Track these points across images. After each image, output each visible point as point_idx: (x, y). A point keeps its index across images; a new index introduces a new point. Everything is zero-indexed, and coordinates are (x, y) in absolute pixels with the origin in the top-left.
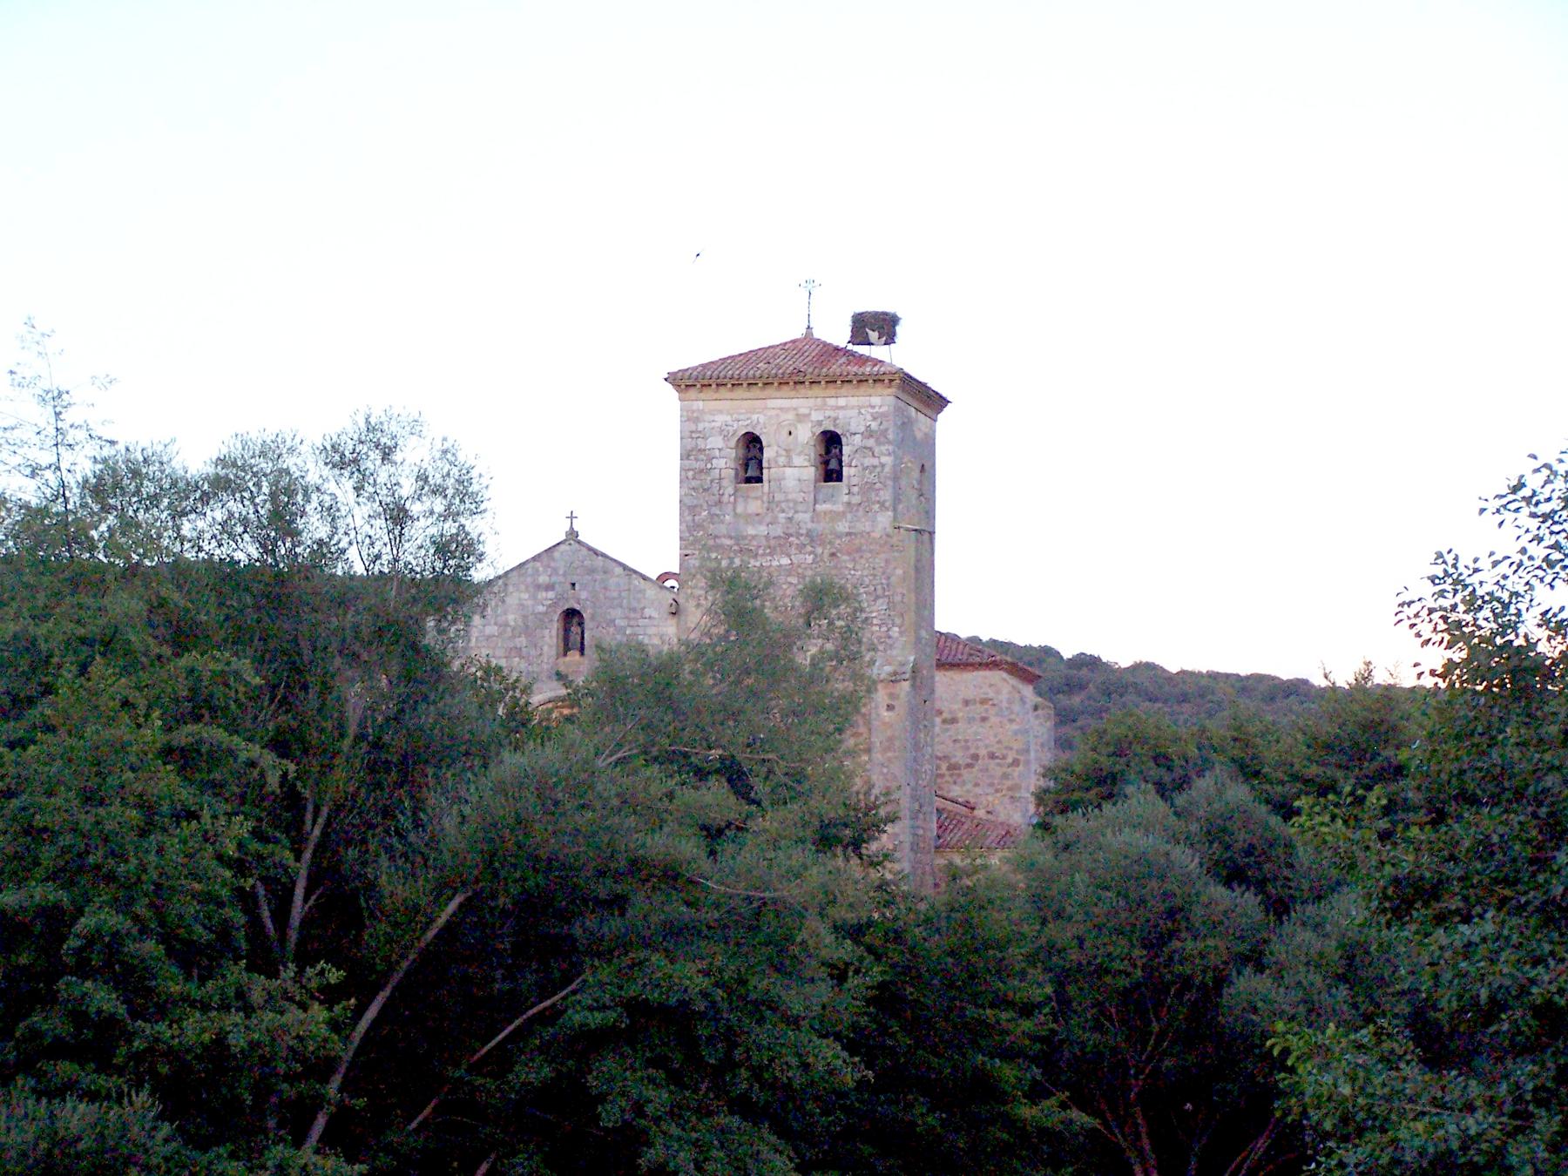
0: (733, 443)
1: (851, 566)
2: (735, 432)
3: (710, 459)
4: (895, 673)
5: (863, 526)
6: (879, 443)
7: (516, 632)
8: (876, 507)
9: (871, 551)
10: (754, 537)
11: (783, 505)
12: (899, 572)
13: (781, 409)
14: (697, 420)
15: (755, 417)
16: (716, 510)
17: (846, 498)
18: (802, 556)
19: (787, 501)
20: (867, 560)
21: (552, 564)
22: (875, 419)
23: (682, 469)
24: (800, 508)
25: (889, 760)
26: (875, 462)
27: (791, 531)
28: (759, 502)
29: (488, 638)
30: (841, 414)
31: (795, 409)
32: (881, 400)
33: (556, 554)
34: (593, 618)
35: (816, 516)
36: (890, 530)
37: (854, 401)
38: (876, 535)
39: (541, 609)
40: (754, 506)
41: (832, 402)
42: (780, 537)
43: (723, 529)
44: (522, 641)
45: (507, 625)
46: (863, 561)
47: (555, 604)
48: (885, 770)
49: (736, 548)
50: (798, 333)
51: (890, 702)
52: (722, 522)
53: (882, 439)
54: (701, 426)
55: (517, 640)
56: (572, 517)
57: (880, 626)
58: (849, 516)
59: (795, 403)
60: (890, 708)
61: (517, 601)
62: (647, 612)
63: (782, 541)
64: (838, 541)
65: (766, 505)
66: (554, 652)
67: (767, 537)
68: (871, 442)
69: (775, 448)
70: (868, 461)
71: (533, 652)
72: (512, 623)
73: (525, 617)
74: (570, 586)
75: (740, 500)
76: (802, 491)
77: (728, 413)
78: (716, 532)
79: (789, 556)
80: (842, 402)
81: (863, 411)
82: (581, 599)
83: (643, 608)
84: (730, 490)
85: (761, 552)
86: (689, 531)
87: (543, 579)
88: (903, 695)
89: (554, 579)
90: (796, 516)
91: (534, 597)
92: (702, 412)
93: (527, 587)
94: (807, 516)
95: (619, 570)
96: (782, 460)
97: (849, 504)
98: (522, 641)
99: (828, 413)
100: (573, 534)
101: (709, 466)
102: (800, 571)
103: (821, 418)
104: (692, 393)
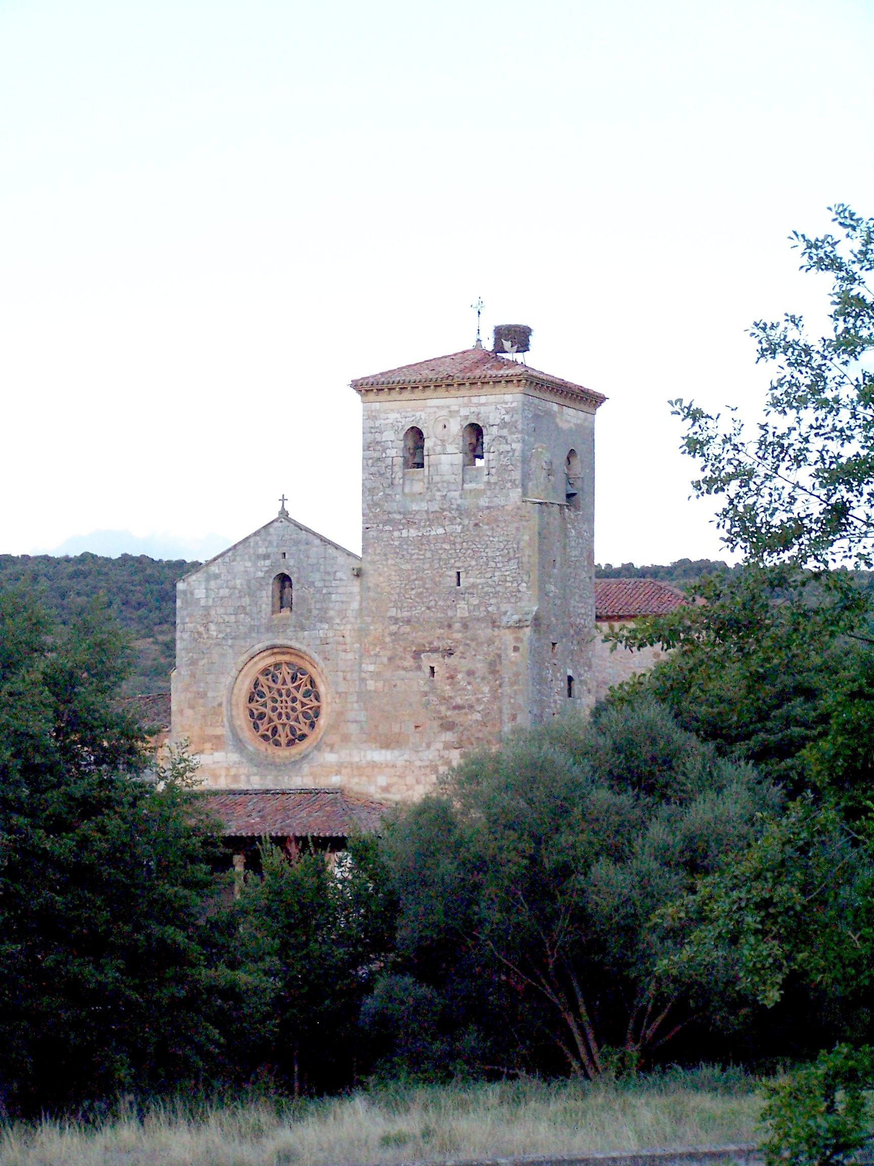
0: (401, 436)
2: (403, 426)
3: (384, 451)
4: (520, 621)
5: (499, 501)
6: (511, 433)
7: (243, 594)
8: (509, 485)
9: (505, 521)
10: (417, 512)
11: (439, 485)
12: (526, 538)
13: (438, 407)
14: (375, 418)
15: (418, 414)
16: (388, 491)
17: (486, 478)
18: (453, 527)
19: (443, 482)
20: (502, 528)
21: (269, 538)
22: (507, 413)
23: (364, 458)
24: (452, 487)
25: (515, 692)
26: (508, 448)
27: (445, 506)
28: (422, 484)
29: (222, 598)
30: (482, 409)
31: (448, 407)
32: (512, 397)
33: (271, 530)
34: (298, 581)
35: (464, 494)
36: (519, 503)
37: (491, 398)
38: (509, 508)
39: (260, 574)
40: (418, 487)
41: (475, 400)
42: (436, 512)
43: (394, 506)
44: (246, 601)
45: (235, 588)
46: (499, 530)
48: (512, 701)
49: (404, 521)
50: (469, 345)
51: (517, 645)
52: (394, 500)
53: (514, 429)
54: (377, 424)
55: (243, 600)
56: (283, 500)
57: (512, 582)
58: (488, 493)
59: (448, 401)
60: (516, 649)
61: (242, 569)
62: (339, 575)
63: (438, 515)
64: (480, 514)
65: (426, 486)
66: (269, 609)
67: (427, 512)
68: (505, 432)
69: (433, 439)
70: (504, 447)
71: (255, 610)
72: (239, 587)
73: (249, 581)
74: (281, 556)
75: (407, 482)
77: (399, 412)
78: (390, 509)
79: (444, 527)
80: (483, 399)
81: (499, 406)
82: (289, 567)
83: (336, 572)
84: (400, 475)
85: (422, 524)
86: (370, 509)
87: (262, 550)
88: (525, 638)
89: (269, 550)
90: (449, 494)
91: (255, 565)
92: (378, 411)
93: (250, 557)
94: (456, 494)
95: (317, 542)
96: (438, 449)
97: (488, 483)
98: (246, 601)
99: (473, 409)
100: (284, 514)
101: (384, 455)
102: (452, 538)
104: (371, 396)
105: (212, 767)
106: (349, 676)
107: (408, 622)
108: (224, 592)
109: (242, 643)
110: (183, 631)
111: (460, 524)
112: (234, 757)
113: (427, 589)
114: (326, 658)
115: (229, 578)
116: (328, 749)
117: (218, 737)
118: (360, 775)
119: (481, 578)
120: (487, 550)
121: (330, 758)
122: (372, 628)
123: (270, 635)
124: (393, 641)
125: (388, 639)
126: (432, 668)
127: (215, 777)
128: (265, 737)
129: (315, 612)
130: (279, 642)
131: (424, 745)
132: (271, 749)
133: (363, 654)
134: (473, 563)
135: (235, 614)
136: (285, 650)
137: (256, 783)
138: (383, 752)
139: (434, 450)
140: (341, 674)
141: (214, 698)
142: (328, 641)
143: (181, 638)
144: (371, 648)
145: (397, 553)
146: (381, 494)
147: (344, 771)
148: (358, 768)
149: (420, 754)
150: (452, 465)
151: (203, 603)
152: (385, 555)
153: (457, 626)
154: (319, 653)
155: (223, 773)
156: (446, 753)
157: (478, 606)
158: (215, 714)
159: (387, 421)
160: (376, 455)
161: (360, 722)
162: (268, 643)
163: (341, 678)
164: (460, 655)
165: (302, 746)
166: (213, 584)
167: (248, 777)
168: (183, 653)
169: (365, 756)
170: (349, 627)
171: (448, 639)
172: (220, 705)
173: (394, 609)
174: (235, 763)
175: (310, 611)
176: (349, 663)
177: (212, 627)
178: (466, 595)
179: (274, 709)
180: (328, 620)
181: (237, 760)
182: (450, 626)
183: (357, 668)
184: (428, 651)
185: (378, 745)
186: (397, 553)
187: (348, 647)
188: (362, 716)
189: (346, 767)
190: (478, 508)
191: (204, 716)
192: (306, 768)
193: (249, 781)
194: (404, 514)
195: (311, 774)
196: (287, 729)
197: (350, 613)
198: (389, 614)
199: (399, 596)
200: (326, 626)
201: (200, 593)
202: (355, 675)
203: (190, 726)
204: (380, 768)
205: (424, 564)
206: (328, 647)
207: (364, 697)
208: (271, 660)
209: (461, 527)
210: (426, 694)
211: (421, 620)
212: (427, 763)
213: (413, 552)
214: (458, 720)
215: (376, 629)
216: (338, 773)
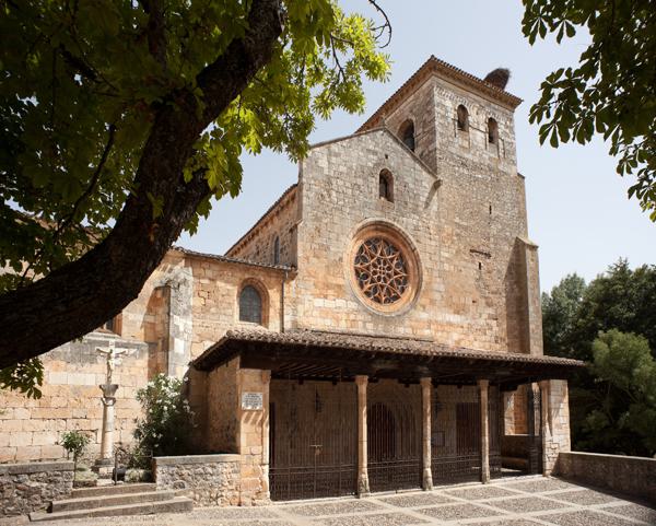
35: (490, 158)
43: (454, 151)
44: (360, 181)
47: (377, 165)
66: (378, 193)
68: (507, 131)
89: (377, 149)
98: (360, 181)
107: (466, 228)
108: (343, 169)
109: (358, 213)
112: (353, 305)
117: (339, 286)
118: (442, 331)
121: (424, 316)
123: (379, 213)
127: (338, 320)
128: (367, 294)
129: (410, 206)
130: (385, 220)
132: (375, 305)
137: (370, 329)
141: (336, 253)
148: (442, 326)
151: (326, 172)
153: (492, 240)
155: (344, 317)
156: (489, 321)
160: (443, 112)
162: (378, 219)
165: (398, 305)
166: (334, 159)
167: (365, 322)
168: (309, 209)
172: (341, 259)
177: (334, 194)
179: (375, 273)
188: (442, 288)
191: (327, 267)
192: (407, 323)
193: (364, 327)
195: (411, 326)
201: (323, 163)
202: (437, 259)
206: (419, 233)
207: (443, 274)
208: (374, 234)
210: (477, 280)
214: (495, 301)
215: (448, 229)
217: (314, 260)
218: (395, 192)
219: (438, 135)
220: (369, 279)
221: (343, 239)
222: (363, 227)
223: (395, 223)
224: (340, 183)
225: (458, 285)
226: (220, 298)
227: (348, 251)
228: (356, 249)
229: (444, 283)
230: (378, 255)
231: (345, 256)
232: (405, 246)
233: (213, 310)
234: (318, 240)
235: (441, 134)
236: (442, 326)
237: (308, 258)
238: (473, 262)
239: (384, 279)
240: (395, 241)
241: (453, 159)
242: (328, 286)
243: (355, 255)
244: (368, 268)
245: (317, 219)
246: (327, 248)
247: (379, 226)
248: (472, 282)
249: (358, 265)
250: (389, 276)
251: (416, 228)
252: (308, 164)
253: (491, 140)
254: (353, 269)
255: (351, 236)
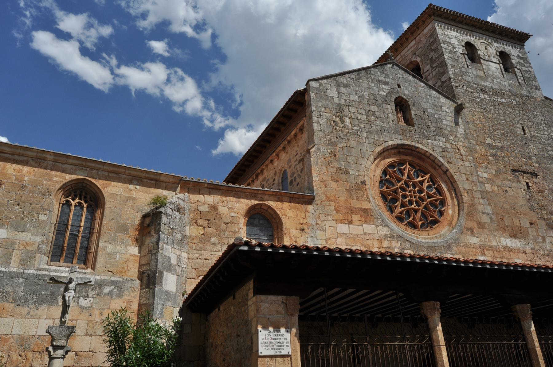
1: (533, 110)
2: (462, 40)
6: (526, 63)
16: (463, 69)
26: (527, 69)
27: (502, 88)
29: (353, 101)
43: (468, 79)
44: (374, 108)
45: (362, 97)
47: (390, 94)
63: (499, 91)
68: (522, 61)
71: (382, 116)
76: (499, 73)
79: (505, 99)
83: (441, 106)
89: (387, 80)
90: (501, 82)
94: (507, 83)
98: (374, 108)
103: (498, 46)
105: (363, 237)
106: (470, 179)
107: (501, 149)
109: (376, 137)
110: (319, 117)
111: (514, 100)
112: (384, 231)
113: (507, 131)
114: (449, 162)
115: (357, 89)
116: (469, 233)
117: (366, 211)
119: (537, 133)
120: (535, 118)
121: (474, 240)
122: (478, 148)
123: (400, 137)
124: (496, 159)
125: (491, 158)
126: (527, 183)
128: (400, 219)
129: (433, 129)
130: (408, 143)
131: (540, 238)
132: (410, 230)
133: (477, 164)
134: (530, 123)
135: (367, 115)
136: (409, 151)
138: (513, 240)
139: (485, 58)
140: (464, 175)
141: (357, 176)
142: (448, 151)
143: (318, 123)
144: (481, 161)
145: (481, 106)
146: (459, 70)
147: (486, 252)
148: (498, 251)
149: (541, 245)
150: (497, 68)
151: (336, 100)
152: (473, 105)
154: (443, 158)
157: (542, 149)
158: (360, 190)
159: (451, 34)
161: (488, 214)
162: (400, 142)
163: (466, 180)
164: (542, 178)
166: (343, 90)
168: (321, 134)
169: (500, 242)
170: (461, 144)
171: (530, 165)
172: (363, 183)
173: (490, 139)
174: (386, 236)
175: (428, 127)
176: (468, 169)
177: (347, 120)
178: (533, 141)
180: (444, 136)
181: (388, 233)
182: (530, 158)
183: (474, 173)
184: (520, 171)
185: (507, 234)
186: (481, 106)
187: (464, 157)
188: (489, 209)
189: (487, 250)
190: (522, 94)
194: (478, 85)
196: (419, 214)
197: (458, 135)
198: (487, 142)
199: (490, 132)
200: (444, 140)
203: (335, 196)
204: (514, 253)
205: (500, 116)
206: (449, 155)
209: (515, 102)
210: (529, 200)
211: (510, 150)
212: (546, 252)
213: (491, 108)
215: (481, 150)
216: (483, 254)
217: (334, 184)
218: (414, 116)
219: (450, 67)
220: (399, 203)
221: (362, 162)
222: (384, 150)
223: (420, 146)
224: (352, 110)
225: (507, 207)
226: (223, 226)
227: (371, 175)
228: (379, 172)
229: (489, 204)
230: (405, 177)
231: (367, 179)
232: (434, 168)
233: (213, 240)
234: (336, 164)
235: (453, 66)
236: (497, 250)
237: (325, 182)
238: (519, 182)
239: (416, 202)
240: (422, 163)
241: (471, 87)
242: (353, 211)
243: (378, 179)
244: (395, 191)
245: (331, 143)
246: (347, 172)
247: (400, 149)
248: (523, 202)
249: (384, 189)
250: (422, 199)
251: (445, 150)
252: (316, 94)
253: (507, 70)
254: (379, 194)
255: (372, 158)
